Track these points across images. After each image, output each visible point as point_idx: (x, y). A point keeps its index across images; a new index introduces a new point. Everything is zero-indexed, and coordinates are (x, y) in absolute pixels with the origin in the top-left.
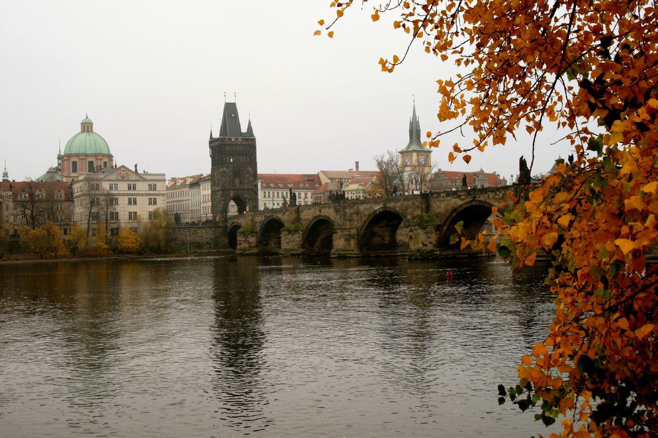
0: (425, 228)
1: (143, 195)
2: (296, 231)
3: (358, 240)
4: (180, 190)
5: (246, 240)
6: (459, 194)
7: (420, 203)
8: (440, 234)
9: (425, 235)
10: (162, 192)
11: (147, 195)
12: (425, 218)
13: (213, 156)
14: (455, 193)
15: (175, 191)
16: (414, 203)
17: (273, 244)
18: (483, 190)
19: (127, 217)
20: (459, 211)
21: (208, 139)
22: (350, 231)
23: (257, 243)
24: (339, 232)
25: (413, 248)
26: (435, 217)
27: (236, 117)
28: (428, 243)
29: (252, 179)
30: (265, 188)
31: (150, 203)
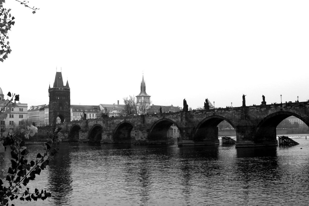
0: (142, 131)
1: (16, 113)
2: (86, 131)
3: (113, 135)
5: (63, 135)
6: (157, 115)
7: (140, 119)
9: (142, 134)
11: (18, 113)
14: (156, 115)
15: (33, 112)
16: (138, 119)
17: (76, 137)
18: (168, 114)
19: (9, 123)
20: (157, 123)
21: (48, 88)
23: (68, 137)
25: (137, 139)
26: (147, 126)
27: (61, 79)
28: (143, 137)
30: (74, 111)
31: (20, 117)
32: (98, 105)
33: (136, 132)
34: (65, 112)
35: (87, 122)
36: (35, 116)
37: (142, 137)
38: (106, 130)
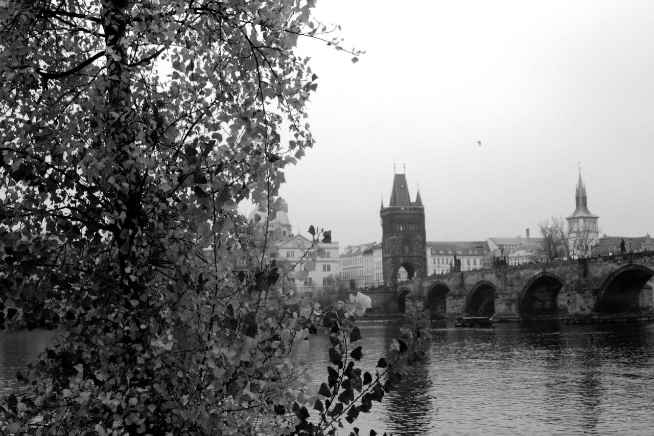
0: (582, 293)
2: (460, 296)
3: (519, 304)
4: (355, 257)
5: (413, 305)
6: (616, 258)
8: (598, 298)
9: (583, 300)
10: (335, 259)
12: (583, 283)
13: (384, 225)
14: (612, 258)
15: (350, 258)
18: (639, 255)
20: (616, 275)
21: (379, 208)
22: (511, 296)
24: (500, 296)
25: (571, 312)
26: (593, 282)
27: (406, 188)
28: (586, 307)
29: (421, 246)
30: (435, 255)
31: (324, 270)
32: (485, 240)
33: (569, 295)
34: (417, 257)
35: (462, 276)
36: (355, 265)
37: (583, 308)
38: (505, 292)
